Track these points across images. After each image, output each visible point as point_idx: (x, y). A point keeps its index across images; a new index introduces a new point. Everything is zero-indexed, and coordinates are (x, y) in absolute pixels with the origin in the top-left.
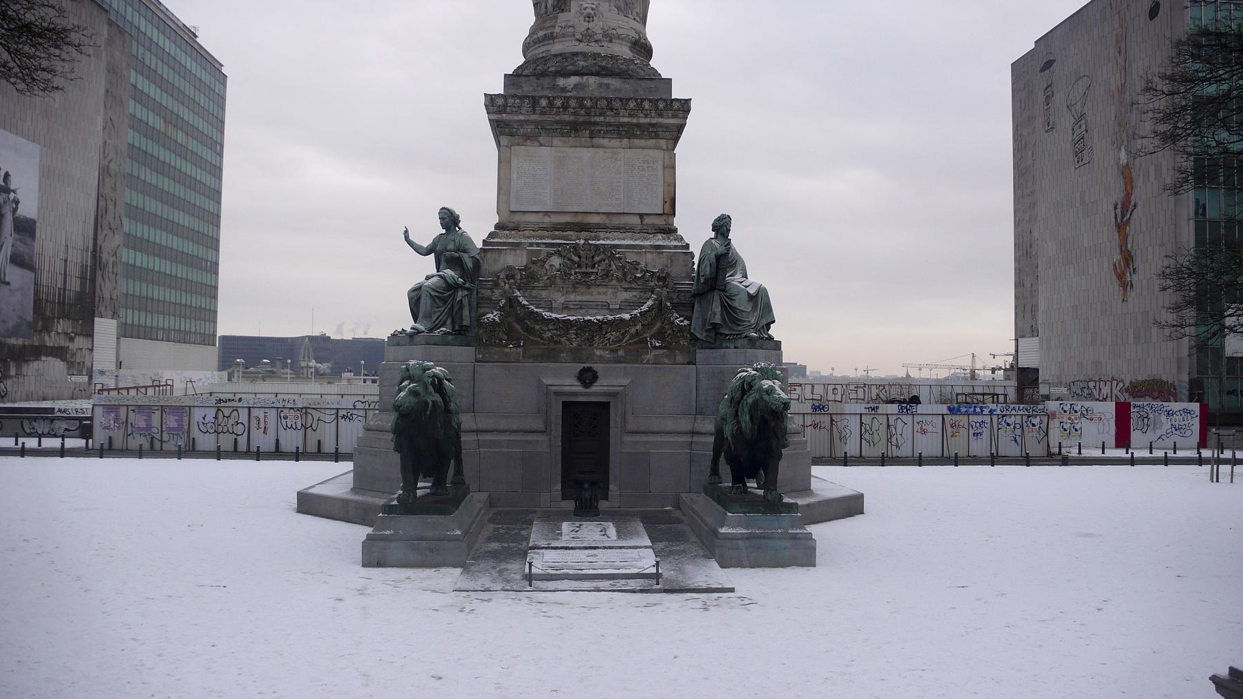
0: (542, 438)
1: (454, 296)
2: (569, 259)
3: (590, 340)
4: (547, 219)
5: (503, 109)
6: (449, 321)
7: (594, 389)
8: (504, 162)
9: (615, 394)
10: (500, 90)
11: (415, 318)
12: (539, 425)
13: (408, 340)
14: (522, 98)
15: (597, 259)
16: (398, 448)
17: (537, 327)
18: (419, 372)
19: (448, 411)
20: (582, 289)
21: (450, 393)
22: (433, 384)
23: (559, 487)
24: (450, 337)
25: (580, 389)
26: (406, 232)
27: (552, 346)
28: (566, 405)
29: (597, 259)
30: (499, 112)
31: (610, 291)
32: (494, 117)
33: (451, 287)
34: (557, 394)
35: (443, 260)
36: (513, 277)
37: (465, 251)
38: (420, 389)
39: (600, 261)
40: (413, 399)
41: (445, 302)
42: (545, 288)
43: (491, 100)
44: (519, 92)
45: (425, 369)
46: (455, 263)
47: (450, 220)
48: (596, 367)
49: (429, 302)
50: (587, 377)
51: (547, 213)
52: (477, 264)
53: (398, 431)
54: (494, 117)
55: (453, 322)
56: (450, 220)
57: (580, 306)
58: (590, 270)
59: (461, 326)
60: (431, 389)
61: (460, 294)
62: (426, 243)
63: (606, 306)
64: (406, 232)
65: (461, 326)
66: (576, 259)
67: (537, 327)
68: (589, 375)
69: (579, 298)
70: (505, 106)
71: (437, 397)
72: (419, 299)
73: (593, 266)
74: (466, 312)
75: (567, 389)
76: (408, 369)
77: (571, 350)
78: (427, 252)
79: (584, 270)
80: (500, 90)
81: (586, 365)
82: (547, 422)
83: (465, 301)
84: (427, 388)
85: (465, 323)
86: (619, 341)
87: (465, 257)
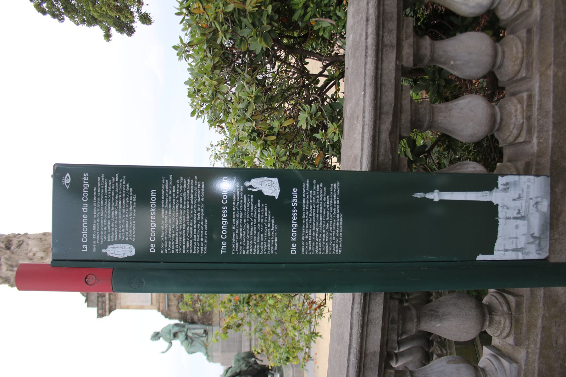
1: (191, 338)
5: (103, 309)
8: (128, 307)
10: (94, 310)
14: (98, 301)
26: (163, 352)
30: (105, 311)
32: (107, 313)
33: (187, 337)
37: (170, 331)
43: (100, 315)
44: (96, 301)
47: (156, 336)
54: (107, 313)
55: (202, 337)
56: (156, 336)
61: (190, 334)
62: (167, 344)
64: (163, 352)
70: (102, 309)
78: (171, 343)
80: (94, 310)
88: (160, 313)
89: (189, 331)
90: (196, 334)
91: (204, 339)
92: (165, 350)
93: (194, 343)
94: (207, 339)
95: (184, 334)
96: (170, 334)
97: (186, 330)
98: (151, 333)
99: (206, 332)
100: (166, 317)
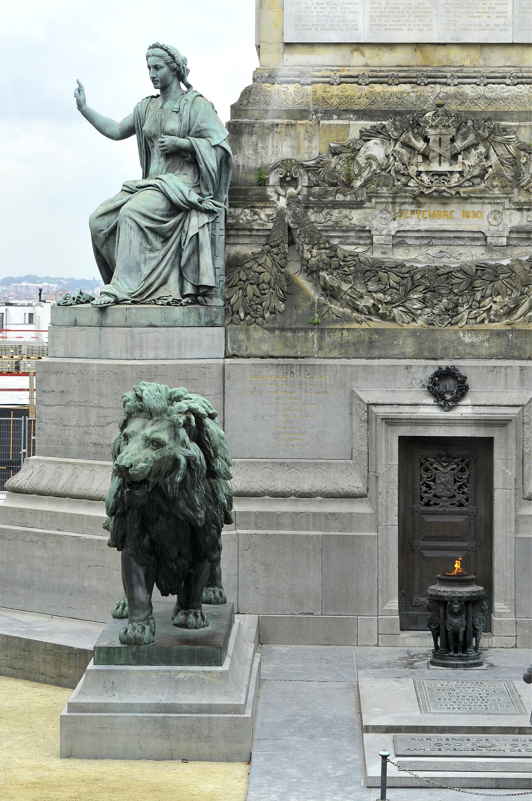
0: (360, 508)
1: (179, 226)
2: (406, 145)
3: (452, 311)
4: (358, 62)
6: (174, 277)
7: (463, 411)
9: (503, 423)
11: (107, 269)
12: (354, 483)
13: (96, 317)
15: (459, 144)
16: (118, 541)
17: (345, 287)
18: (163, 404)
19: (212, 474)
20: (435, 207)
21: (216, 440)
22: (187, 424)
23: (394, 604)
24: (177, 312)
25: (435, 412)
27: (376, 323)
28: (405, 443)
29: (459, 144)
31: (488, 208)
33: (177, 209)
34: (391, 422)
35: (156, 152)
36: (294, 182)
37: (200, 134)
38: (164, 436)
39: (467, 149)
40: (151, 454)
41: (166, 240)
42: (358, 205)
45: (173, 399)
46: (183, 157)
47: (169, 73)
48: (465, 366)
49: (136, 238)
50: (448, 386)
51: (358, 46)
52: (225, 160)
53: (120, 510)
55: (182, 278)
56: (169, 73)
57: (430, 237)
58: (445, 167)
59: (197, 287)
60: (183, 432)
61: (195, 222)
62: (120, 115)
63: (480, 238)
65: (197, 287)
66: (420, 145)
67: (345, 287)
68: (450, 384)
69: (425, 224)
71: (194, 450)
72: (114, 231)
73: (454, 157)
74: (206, 258)
75: (406, 412)
76: (140, 398)
77: (414, 333)
78: (126, 134)
79: (435, 167)
81: (444, 363)
82: (371, 476)
83: (205, 238)
84: (176, 435)
85: (207, 280)
86: (510, 312)
87: (203, 147)
88: (249, 82)
89: (205, 219)
90: (197, 249)
91: (172, 290)
92: (90, 105)
93: (156, 243)
94: (176, 303)
95: (194, 198)
96: (186, 133)
97: (208, 205)
98: (183, 50)
99: (201, 294)
100: (233, 107)
